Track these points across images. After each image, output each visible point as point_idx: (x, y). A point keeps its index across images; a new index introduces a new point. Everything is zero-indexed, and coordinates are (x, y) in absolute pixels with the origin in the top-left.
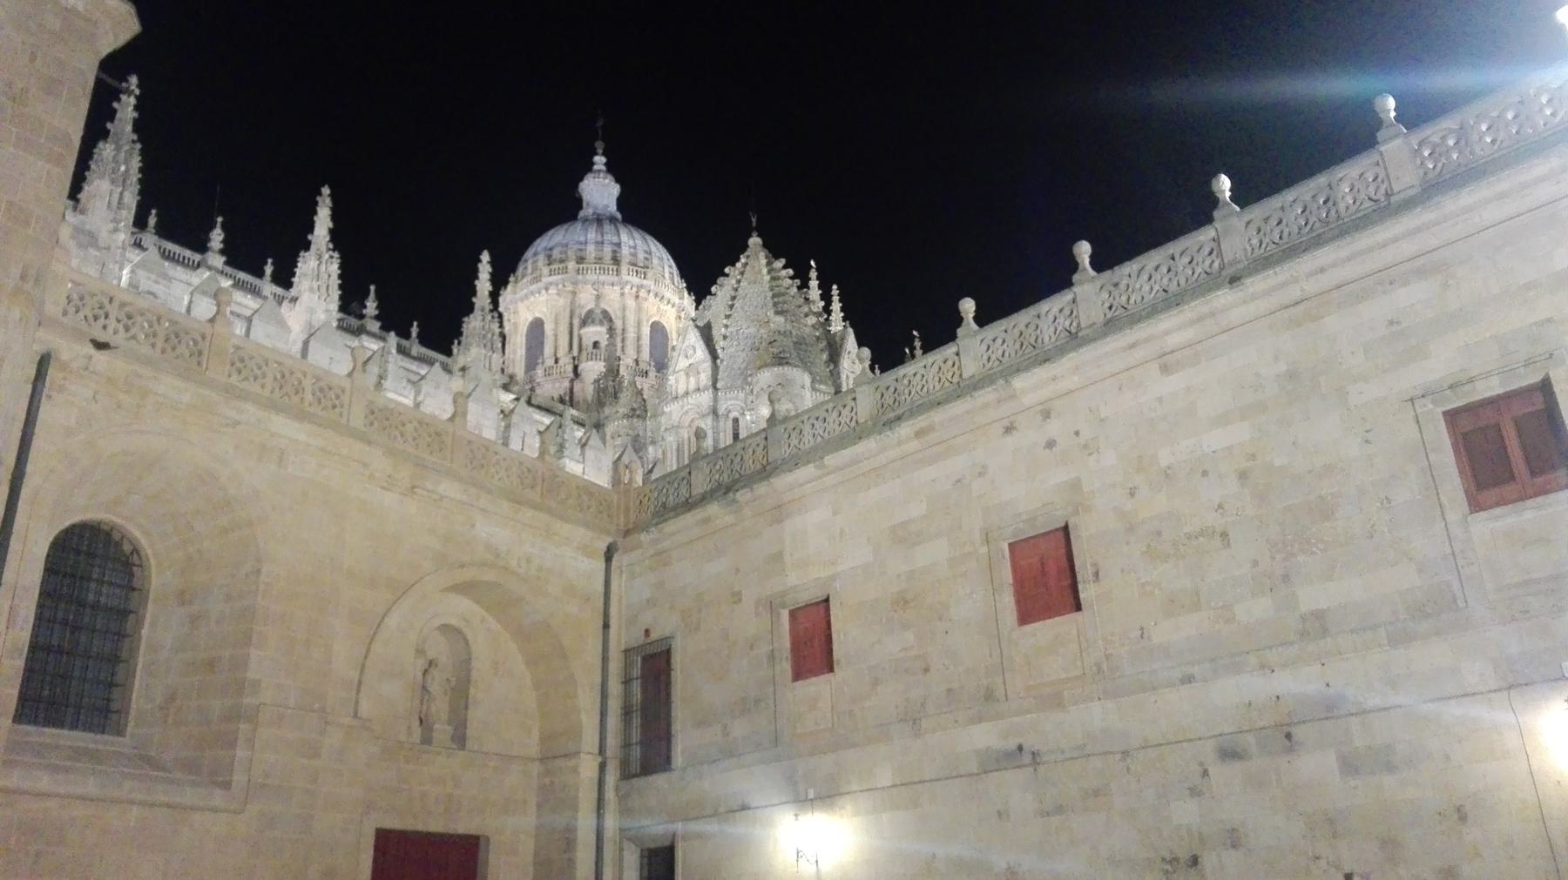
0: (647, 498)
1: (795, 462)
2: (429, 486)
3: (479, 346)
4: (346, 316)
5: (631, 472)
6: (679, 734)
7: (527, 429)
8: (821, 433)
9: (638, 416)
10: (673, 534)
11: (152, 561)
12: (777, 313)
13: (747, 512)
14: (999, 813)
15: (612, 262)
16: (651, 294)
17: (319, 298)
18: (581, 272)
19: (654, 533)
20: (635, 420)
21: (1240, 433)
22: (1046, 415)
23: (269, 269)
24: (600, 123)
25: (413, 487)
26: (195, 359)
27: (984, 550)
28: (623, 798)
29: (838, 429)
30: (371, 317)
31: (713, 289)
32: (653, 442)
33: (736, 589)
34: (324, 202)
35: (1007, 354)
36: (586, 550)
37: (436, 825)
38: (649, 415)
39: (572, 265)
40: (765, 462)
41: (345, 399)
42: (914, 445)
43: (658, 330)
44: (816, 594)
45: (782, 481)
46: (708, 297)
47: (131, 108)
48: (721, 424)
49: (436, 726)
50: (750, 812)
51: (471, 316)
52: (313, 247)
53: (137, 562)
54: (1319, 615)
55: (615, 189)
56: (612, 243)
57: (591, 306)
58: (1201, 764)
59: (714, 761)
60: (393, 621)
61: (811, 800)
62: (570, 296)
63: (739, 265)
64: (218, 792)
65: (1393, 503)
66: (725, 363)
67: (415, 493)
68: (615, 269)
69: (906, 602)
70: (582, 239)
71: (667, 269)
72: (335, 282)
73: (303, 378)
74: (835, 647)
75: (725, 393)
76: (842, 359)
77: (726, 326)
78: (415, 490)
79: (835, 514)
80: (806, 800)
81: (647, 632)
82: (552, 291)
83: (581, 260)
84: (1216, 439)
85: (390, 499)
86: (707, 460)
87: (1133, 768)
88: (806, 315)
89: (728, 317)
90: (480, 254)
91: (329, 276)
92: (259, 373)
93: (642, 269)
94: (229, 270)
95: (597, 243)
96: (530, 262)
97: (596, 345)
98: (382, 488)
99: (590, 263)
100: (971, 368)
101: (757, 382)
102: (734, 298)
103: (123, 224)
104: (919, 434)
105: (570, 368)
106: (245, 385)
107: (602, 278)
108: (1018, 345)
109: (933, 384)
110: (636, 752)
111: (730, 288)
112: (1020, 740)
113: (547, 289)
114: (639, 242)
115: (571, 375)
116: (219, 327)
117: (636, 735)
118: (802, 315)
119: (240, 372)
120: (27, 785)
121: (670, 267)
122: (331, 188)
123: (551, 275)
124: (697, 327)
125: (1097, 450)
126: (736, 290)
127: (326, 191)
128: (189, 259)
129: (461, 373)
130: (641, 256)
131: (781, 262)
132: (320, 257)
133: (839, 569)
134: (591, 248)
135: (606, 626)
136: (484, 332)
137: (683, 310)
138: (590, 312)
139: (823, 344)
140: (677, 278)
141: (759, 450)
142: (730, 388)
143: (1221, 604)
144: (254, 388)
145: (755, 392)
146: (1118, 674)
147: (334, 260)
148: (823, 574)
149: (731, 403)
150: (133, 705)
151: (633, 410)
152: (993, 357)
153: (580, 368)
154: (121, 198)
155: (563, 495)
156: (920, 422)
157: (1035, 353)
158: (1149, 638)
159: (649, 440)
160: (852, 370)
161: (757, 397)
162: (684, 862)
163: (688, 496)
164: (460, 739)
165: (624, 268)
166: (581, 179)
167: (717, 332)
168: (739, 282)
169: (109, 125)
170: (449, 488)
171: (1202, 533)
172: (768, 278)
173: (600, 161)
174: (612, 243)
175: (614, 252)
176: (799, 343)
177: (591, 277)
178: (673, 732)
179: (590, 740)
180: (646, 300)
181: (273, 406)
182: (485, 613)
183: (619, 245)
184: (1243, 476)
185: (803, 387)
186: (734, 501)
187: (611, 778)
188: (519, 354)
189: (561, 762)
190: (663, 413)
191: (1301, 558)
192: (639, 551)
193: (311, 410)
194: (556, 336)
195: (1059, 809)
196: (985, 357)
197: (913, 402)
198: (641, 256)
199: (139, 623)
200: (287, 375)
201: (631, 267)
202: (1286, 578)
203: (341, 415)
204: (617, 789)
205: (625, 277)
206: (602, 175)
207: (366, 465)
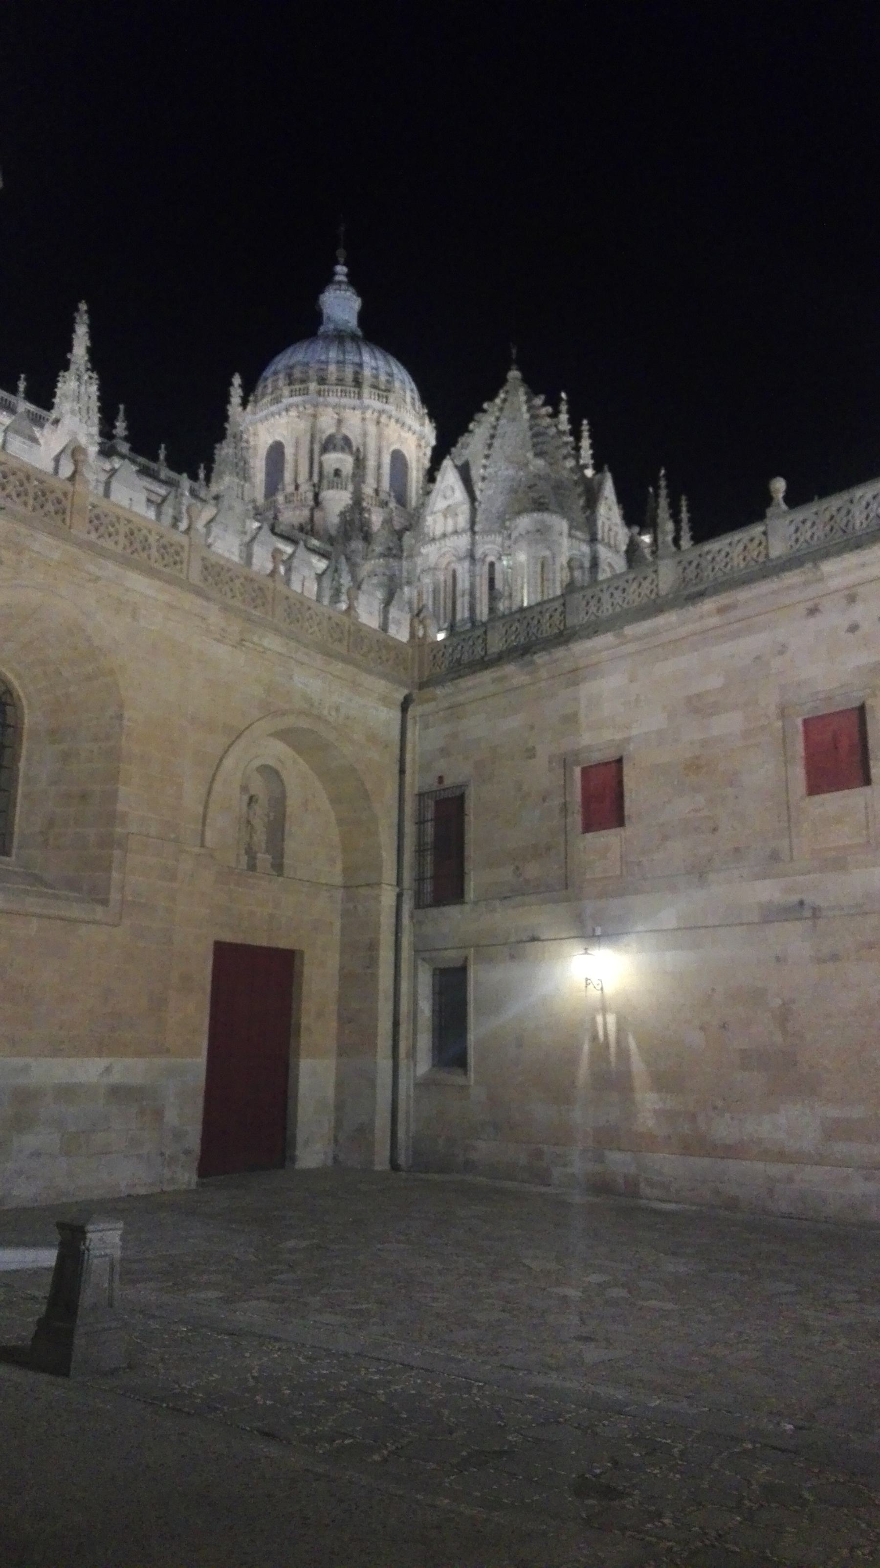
0: (441, 653)
1: (594, 629)
2: (255, 639)
3: (231, 474)
4: (106, 441)
5: (425, 627)
6: (472, 873)
7: (306, 572)
8: (621, 603)
9: (395, 556)
10: (469, 689)
11: (24, 702)
12: (537, 455)
13: (543, 673)
14: (778, 959)
15: (354, 384)
17: (80, 420)
18: (322, 393)
19: (449, 688)
20: (391, 560)
22: (852, 599)
23: (22, 385)
25: (242, 640)
26: (59, 518)
27: (779, 724)
28: (418, 923)
29: (638, 600)
30: (121, 438)
31: (471, 426)
32: (409, 583)
34: (81, 319)
35: (815, 538)
36: (385, 700)
37: (262, 940)
38: (405, 554)
39: (313, 386)
40: (562, 627)
41: (185, 555)
42: (715, 620)
43: (398, 459)
44: (610, 755)
45: (579, 647)
46: (466, 435)
48: (478, 568)
49: (259, 855)
50: (540, 943)
51: (224, 442)
52: (73, 367)
53: (9, 701)
55: (356, 303)
56: (353, 363)
57: (331, 430)
59: (505, 898)
60: (229, 763)
61: (599, 936)
63: (498, 401)
64: (99, 909)
66: (483, 506)
67: (244, 646)
68: (356, 391)
70: (323, 358)
71: (408, 394)
72: (95, 404)
73: (148, 534)
74: (627, 804)
76: (599, 505)
77: (485, 467)
78: (244, 642)
80: (594, 936)
81: (441, 779)
82: (293, 413)
83: (322, 381)
85: (222, 651)
86: (503, 621)
88: (565, 458)
89: (487, 457)
90: (231, 375)
91: (89, 397)
92: (111, 529)
93: (384, 392)
95: (338, 362)
97: (337, 473)
98: (218, 641)
99: (331, 385)
100: (778, 549)
101: (516, 527)
102: (492, 437)
104: (721, 610)
105: (310, 496)
106: (102, 542)
107: (345, 401)
108: (828, 528)
109: (737, 560)
110: (428, 887)
111: (489, 426)
113: (287, 410)
114: (381, 363)
115: (312, 503)
116: (79, 487)
117: (429, 872)
118: (561, 457)
119: (97, 529)
121: (412, 390)
122: (87, 303)
123: (291, 396)
124: (456, 467)
126: (495, 428)
127: (83, 307)
130: (383, 378)
131: (540, 399)
132: (79, 378)
133: (634, 732)
134: (332, 368)
135: (402, 771)
136: (235, 460)
137: (424, 438)
138: (331, 438)
139: (580, 489)
140: (418, 404)
141: (557, 616)
144: (108, 544)
145: (513, 536)
147: (93, 381)
148: (618, 736)
149: (488, 547)
150: (16, 829)
151: (390, 549)
152: (802, 539)
155: (365, 649)
156: (723, 599)
157: (845, 538)
159: (404, 581)
160: (608, 516)
161: (515, 542)
163: (483, 653)
164: (278, 867)
165: (366, 391)
166: (322, 292)
167: (476, 472)
168: (498, 419)
170: (272, 642)
172: (526, 416)
174: (353, 363)
176: (558, 487)
177: (332, 399)
178: (466, 870)
179: (389, 874)
180: (387, 426)
181: (126, 562)
182: (296, 756)
183: (360, 365)
185: (561, 534)
186: (532, 663)
187: (407, 906)
189: (363, 891)
190: (420, 554)
192: (433, 704)
193: (156, 566)
195: (835, 957)
196: (794, 537)
197: (716, 579)
198: (383, 378)
199: (16, 758)
200: (136, 532)
201: (373, 390)
203: (181, 571)
204: (412, 917)
205: (367, 401)
206: (343, 287)
207: (204, 619)
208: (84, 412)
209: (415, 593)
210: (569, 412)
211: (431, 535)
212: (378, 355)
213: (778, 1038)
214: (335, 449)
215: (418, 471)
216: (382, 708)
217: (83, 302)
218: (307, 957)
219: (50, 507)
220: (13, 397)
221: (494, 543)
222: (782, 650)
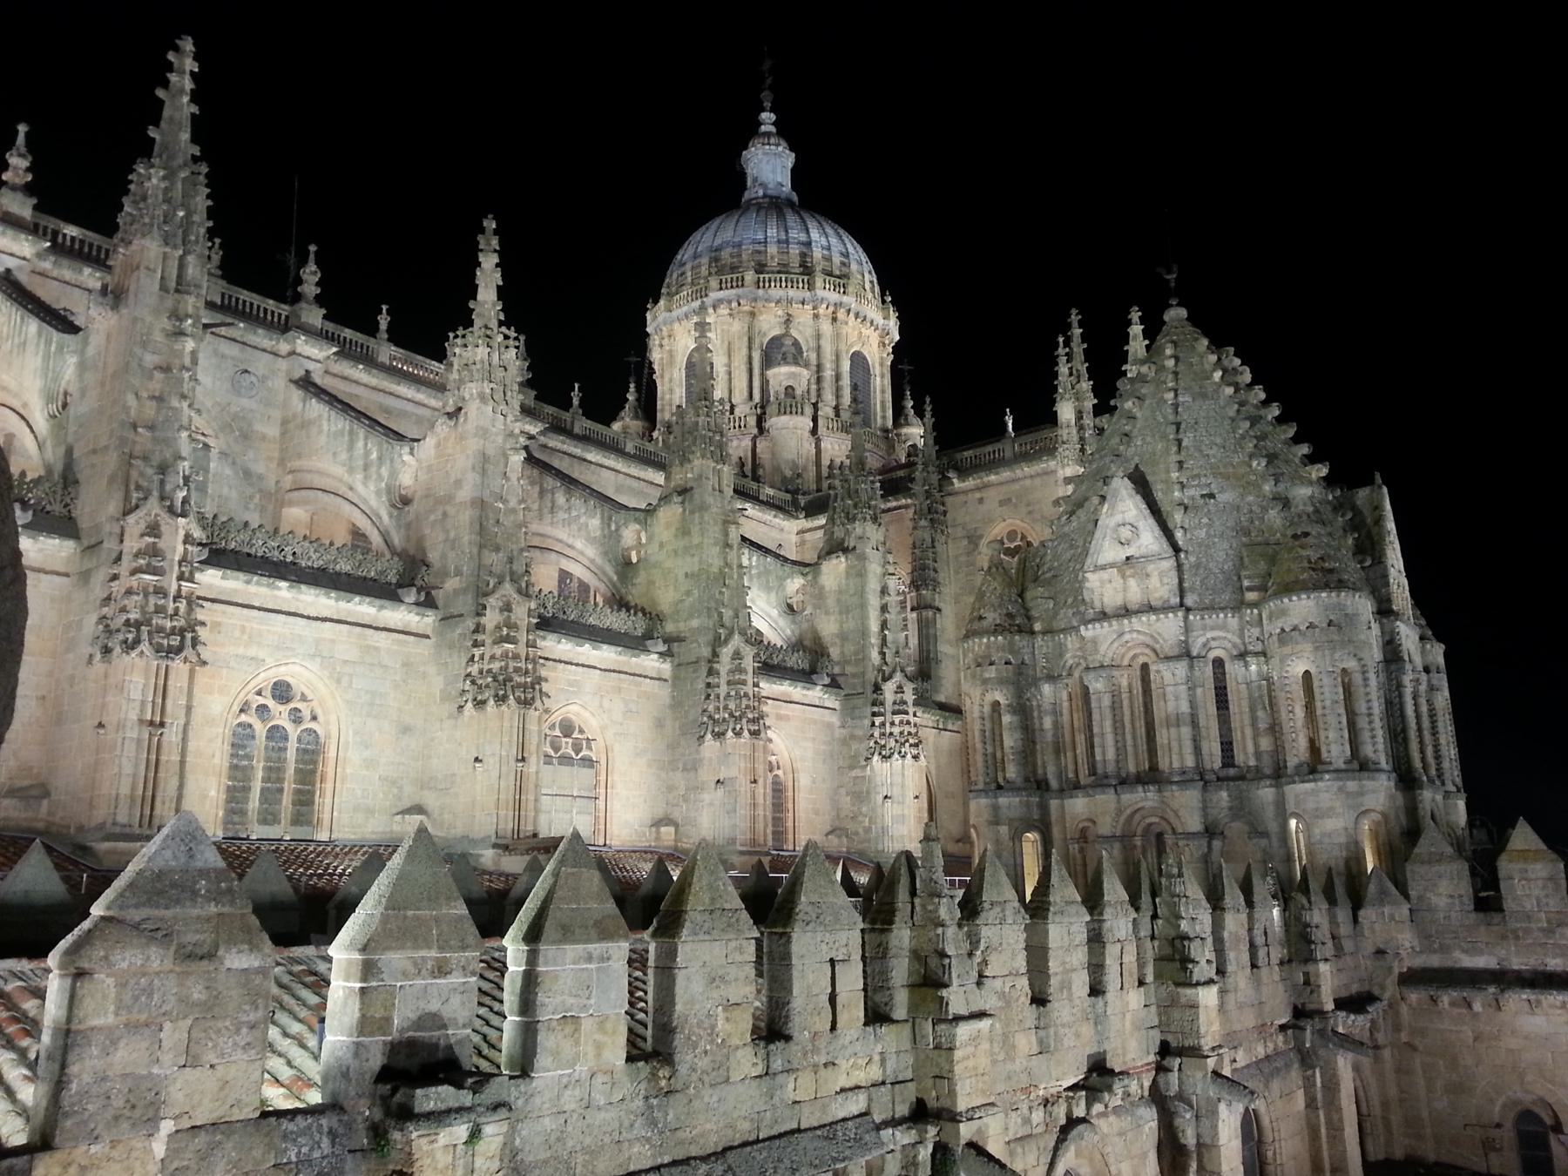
16: (852, 315)
23: (384, 321)
24: (767, 65)
32: (1051, 678)
39: (750, 276)
43: (858, 360)
47: (186, 99)
55: (789, 159)
56: (799, 243)
57: (777, 332)
62: (747, 319)
70: (760, 236)
71: (867, 276)
75: (1203, 618)
82: (723, 310)
83: (760, 268)
93: (840, 279)
94: (330, 327)
95: (779, 242)
96: (688, 266)
97: (790, 390)
99: (773, 272)
103: (190, 321)
105: (752, 421)
107: (792, 293)
113: (715, 308)
114: (834, 240)
115: (755, 431)
123: (721, 289)
127: (490, 224)
128: (273, 312)
129: (680, 499)
130: (837, 259)
134: (772, 249)
138: (775, 342)
142: (1212, 608)
147: (511, 342)
151: (1010, 615)
153: (767, 425)
154: (182, 266)
165: (819, 282)
166: (746, 148)
169: (152, 132)
173: (767, 117)
174: (799, 243)
175: (803, 255)
177: (776, 292)
180: (847, 323)
183: (809, 244)
188: (678, 395)
194: (730, 373)
198: (837, 259)
201: (828, 278)
205: (820, 293)
208: (499, 396)
209: (1065, 696)
210: (1142, 320)
211: (1097, 604)
212: (829, 230)
214: (785, 360)
215: (882, 376)
217: (490, 216)
220: (372, 339)
221: (1224, 627)
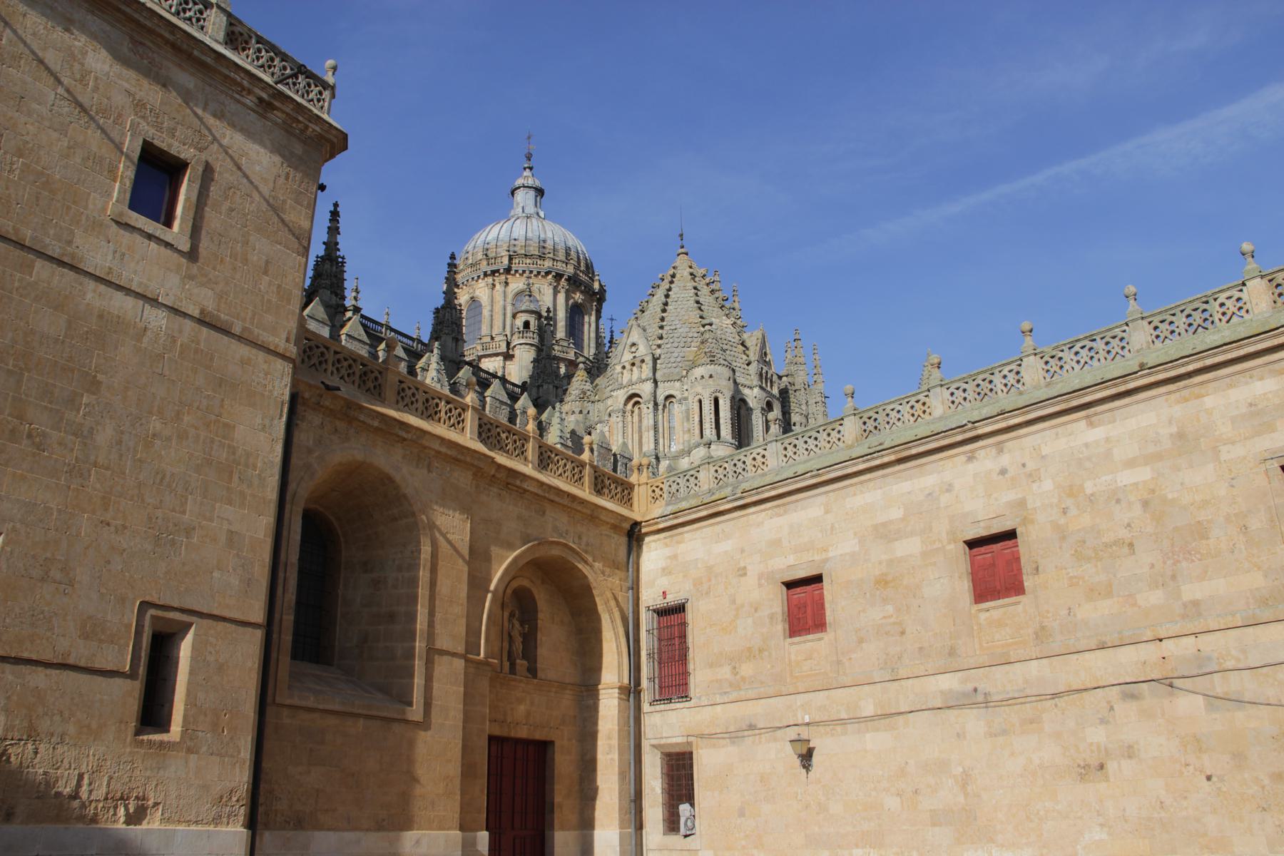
21: (1143, 474)
33: (742, 565)
54: (1196, 603)
58: (1108, 702)
65: (1249, 530)
69: (886, 583)
79: (827, 512)
84: (1126, 478)
87: (1059, 705)
112: (977, 685)
120: (303, 703)
125: (1039, 478)
133: (831, 554)
143: (1127, 593)
146: (1051, 640)
158: (1075, 615)
162: (630, 754)
171: (1116, 543)
184: (1145, 504)
191: (1184, 564)
195: (1004, 732)
202: (1174, 577)
213: (961, 799)
216: (613, 535)
218: (557, 744)
219: (370, 384)
222: (949, 488)
